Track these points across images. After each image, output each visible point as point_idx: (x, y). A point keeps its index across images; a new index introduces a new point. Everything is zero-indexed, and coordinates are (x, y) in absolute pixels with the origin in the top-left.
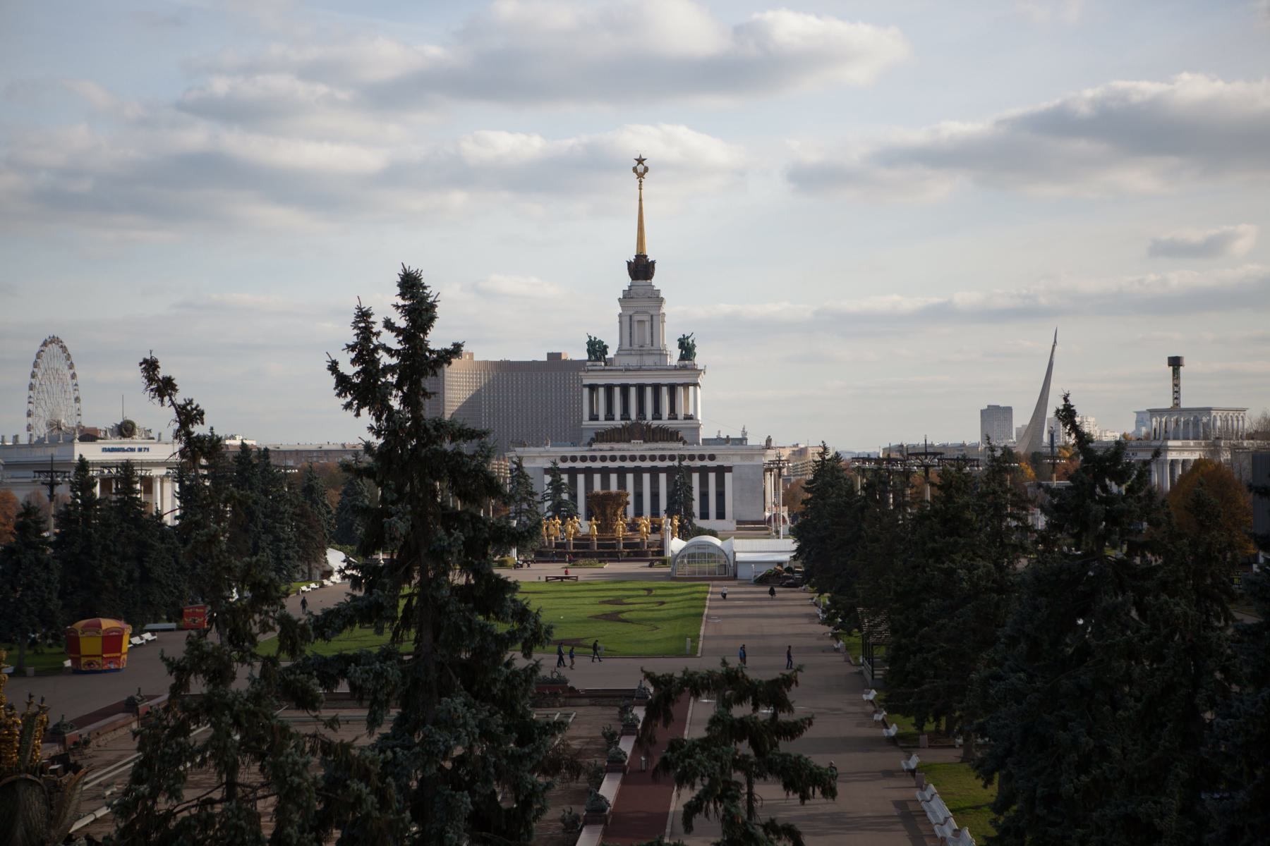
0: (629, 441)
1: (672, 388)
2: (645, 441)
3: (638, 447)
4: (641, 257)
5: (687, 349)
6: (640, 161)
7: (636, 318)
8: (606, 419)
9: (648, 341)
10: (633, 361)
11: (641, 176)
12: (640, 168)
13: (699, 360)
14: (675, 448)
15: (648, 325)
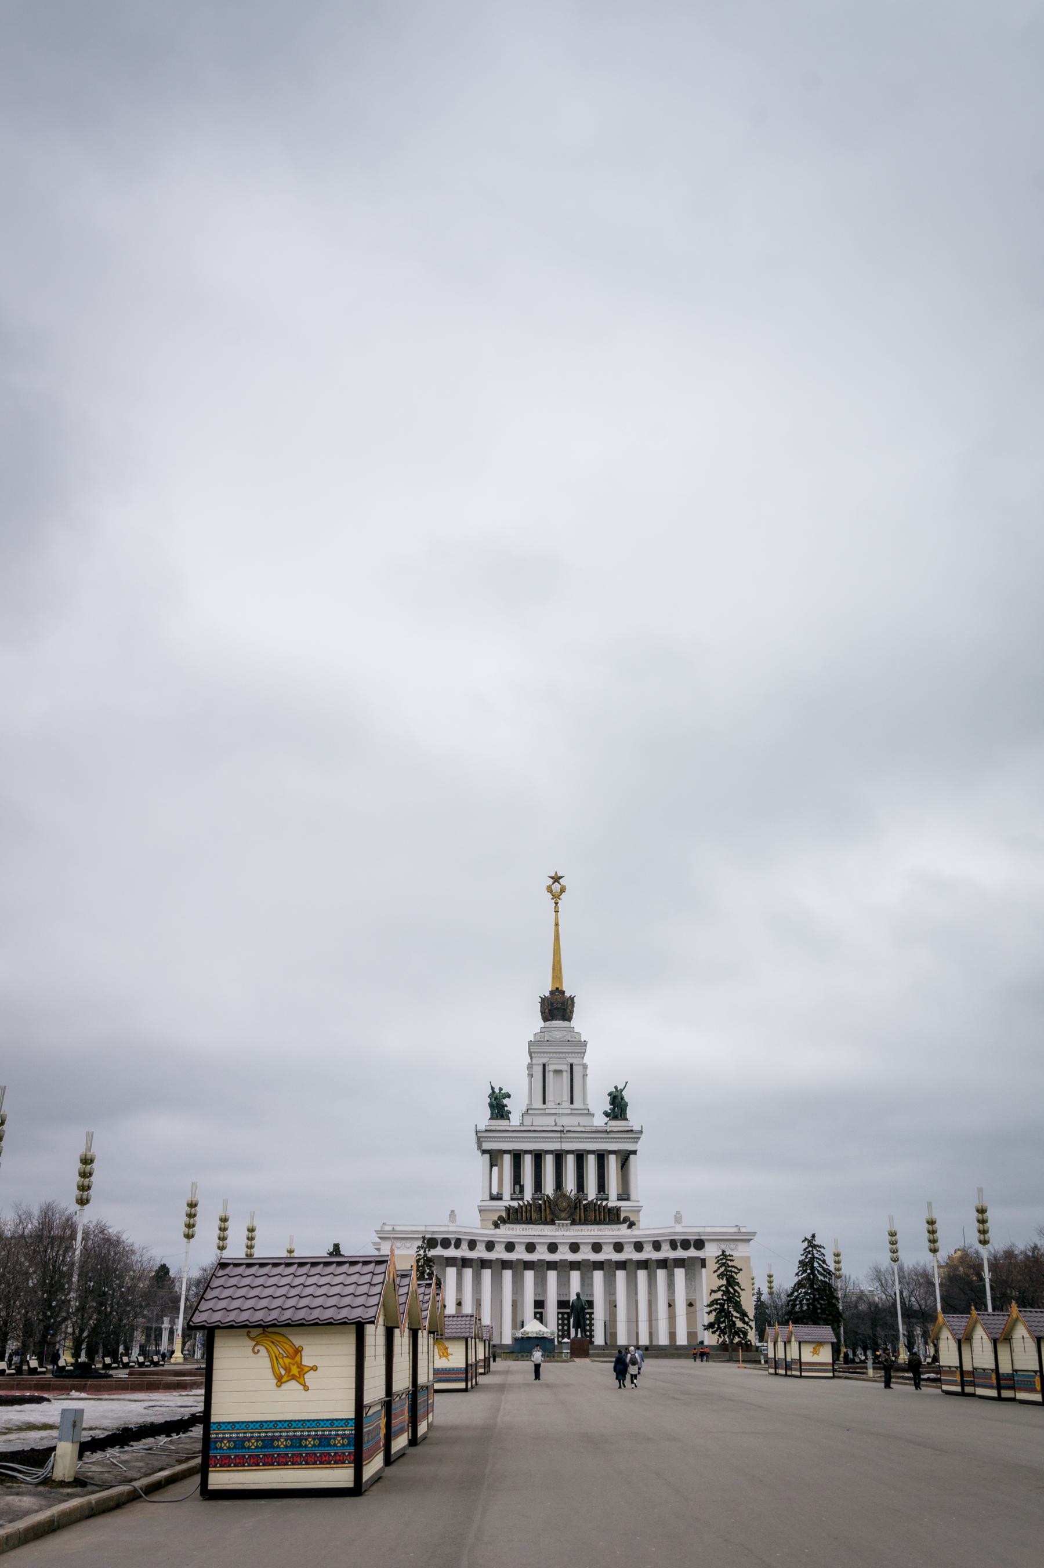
0: (552, 1222)
1: (601, 1157)
2: (573, 1223)
3: (563, 1233)
4: (557, 992)
5: (618, 1106)
6: (556, 879)
7: (550, 1068)
8: (512, 1199)
9: (566, 1096)
10: (547, 1122)
11: (556, 897)
12: (556, 887)
13: (635, 1118)
14: (620, 1232)
15: (566, 1076)
